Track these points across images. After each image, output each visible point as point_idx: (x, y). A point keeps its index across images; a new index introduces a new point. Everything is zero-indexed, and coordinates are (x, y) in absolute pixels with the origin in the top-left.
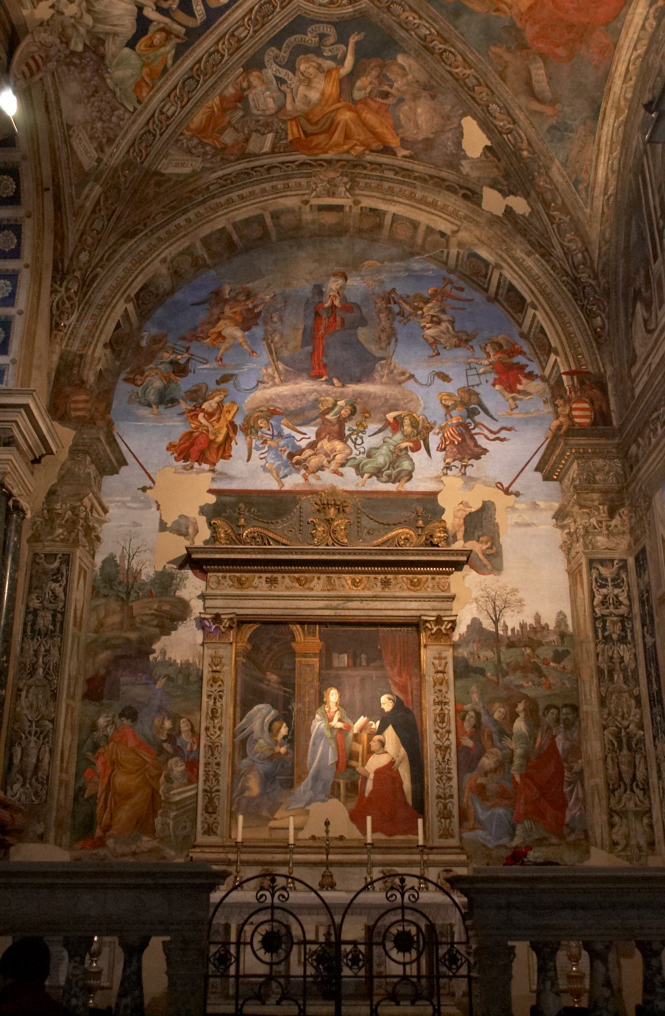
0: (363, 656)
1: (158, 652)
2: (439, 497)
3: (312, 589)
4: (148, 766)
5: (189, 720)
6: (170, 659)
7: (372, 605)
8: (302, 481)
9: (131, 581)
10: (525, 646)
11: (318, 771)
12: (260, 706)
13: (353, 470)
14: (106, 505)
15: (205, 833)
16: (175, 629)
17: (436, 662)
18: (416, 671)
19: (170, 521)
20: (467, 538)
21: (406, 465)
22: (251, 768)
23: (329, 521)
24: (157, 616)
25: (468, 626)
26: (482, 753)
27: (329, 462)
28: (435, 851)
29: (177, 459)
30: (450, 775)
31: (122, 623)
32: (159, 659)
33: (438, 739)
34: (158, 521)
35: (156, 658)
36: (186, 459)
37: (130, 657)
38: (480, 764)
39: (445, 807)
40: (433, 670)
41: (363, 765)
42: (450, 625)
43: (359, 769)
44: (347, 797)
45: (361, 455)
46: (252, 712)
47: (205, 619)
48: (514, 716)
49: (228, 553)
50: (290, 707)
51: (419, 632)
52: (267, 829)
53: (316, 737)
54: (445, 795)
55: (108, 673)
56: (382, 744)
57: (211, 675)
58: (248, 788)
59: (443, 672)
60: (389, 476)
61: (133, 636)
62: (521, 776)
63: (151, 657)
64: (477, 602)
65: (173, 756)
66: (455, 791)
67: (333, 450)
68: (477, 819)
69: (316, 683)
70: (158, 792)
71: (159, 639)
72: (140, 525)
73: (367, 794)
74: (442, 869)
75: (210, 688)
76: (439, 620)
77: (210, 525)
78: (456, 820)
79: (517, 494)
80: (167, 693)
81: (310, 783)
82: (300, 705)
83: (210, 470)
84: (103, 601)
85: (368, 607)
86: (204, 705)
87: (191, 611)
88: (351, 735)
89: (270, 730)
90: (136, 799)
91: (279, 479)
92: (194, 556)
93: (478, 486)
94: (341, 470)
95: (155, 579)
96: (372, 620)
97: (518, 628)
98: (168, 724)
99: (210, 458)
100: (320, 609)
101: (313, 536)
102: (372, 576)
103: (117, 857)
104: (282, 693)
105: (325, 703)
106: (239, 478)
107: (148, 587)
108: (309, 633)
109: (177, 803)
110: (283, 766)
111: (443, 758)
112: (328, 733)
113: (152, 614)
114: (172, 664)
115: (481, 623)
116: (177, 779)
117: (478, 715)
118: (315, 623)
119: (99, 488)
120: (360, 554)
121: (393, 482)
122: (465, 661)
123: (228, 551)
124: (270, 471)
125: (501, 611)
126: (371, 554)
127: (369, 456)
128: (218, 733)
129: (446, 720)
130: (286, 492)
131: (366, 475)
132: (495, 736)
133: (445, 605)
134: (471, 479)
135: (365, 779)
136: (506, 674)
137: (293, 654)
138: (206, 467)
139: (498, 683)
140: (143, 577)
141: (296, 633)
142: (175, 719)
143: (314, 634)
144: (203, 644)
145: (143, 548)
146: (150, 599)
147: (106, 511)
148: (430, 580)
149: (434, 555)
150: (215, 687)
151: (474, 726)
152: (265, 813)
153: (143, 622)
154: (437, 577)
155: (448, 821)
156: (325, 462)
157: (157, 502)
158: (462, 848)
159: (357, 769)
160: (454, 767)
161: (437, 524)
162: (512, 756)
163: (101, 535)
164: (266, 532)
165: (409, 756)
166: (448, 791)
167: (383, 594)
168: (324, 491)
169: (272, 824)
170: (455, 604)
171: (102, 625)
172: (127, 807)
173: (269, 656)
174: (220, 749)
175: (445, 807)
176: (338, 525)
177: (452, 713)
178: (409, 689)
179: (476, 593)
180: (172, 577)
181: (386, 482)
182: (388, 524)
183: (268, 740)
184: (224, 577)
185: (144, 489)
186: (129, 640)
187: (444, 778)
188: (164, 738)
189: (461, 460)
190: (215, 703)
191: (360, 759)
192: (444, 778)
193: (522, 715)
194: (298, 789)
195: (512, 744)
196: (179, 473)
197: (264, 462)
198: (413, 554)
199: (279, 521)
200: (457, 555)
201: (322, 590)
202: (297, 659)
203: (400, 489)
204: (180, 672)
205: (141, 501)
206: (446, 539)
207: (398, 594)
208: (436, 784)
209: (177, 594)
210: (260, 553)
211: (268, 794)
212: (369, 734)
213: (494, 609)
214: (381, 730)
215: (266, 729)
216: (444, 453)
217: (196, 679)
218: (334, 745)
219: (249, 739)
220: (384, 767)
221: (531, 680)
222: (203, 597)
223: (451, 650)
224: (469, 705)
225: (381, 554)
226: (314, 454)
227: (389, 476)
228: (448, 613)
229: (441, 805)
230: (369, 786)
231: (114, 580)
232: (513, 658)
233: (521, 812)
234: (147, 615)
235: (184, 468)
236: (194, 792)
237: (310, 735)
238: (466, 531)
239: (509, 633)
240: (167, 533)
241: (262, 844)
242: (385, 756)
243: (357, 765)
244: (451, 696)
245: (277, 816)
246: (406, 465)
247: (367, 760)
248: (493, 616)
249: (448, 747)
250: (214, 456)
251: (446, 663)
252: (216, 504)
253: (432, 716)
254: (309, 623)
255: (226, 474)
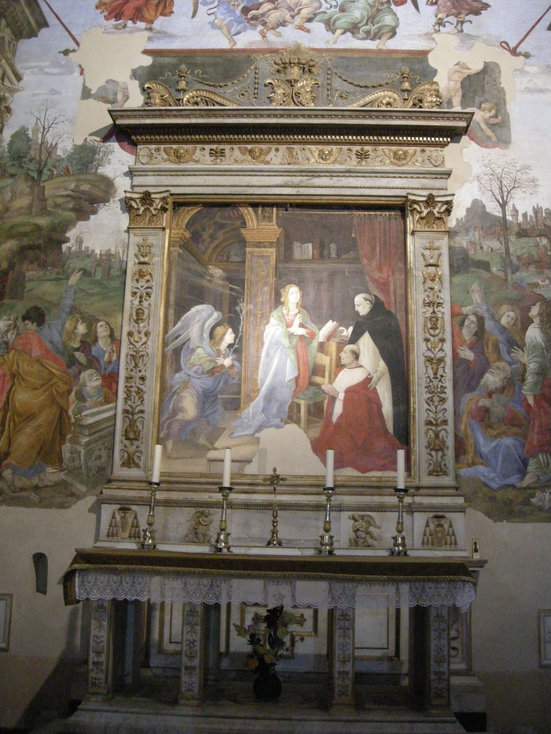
0: (333, 246)
1: (72, 241)
2: (430, 57)
3: (268, 163)
4: (55, 380)
5: (108, 324)
6: (87, 248)
7: (345, 181)
8: (259, 38)
9: (44, 157)
10: (540, 235)
11: (272, 390)
12: (199, 307)
13: (322, 26)
14: (21, 71)
15: (123, 465)
16: (95, 212)
17: (427, 253)
18: (401, 265)
19: (94, 87)
20: (464, 102)
21: (388, 20)
22: (186, 384)
23: (291, 83)
24: (73, 198)
25: (468, 210)
26: (485, 367)
27: (293, 17)
28: (422, 491)
29: (106, 18)
30: (443, 395)
31: (30, 206)
32: (73, 249)
33: (429, 349)
34: (80, 88)
35: (69, 248)
36: (118, 17)
37: (38, 247)
38: (483, 381)
39: (437, 435)
40: (424, 263)
41: (331, 382)
42: (445, 207)
43: (326, 387)
44: (309, 422)
45: (333, 9)
46: (188, 314)
47: (131, 199)
48: (526, 322)
49: (161, 116)
50: (238, 309)
51: (404, 217)
52: (205, 461)
53: (269, 347)
54: (436, 420)
55: (11, 266)
56: (356, 355)
57: (138, 267)
58: (182, 410)
59: (436, 266)
60: (368, 33)
61: (43, 221)
62: (535, 396)
63: (64, 247)
64: (478, 180)
65: (86, 368)
66: (450, 416)
67: (297, 5)
68: (478, 453)
69: (272, 280)
70: (67, 412)
71: (74, 225)
72: (60, 93)
73: (334, 419)
74: (432, 514)
75: (136, 285)
76: (430, 201)
77: (144, 90)
78: (450, 453)
79: (527, 56)
80: (82, 290)
81: (261, 405)
82: (251, 306)
83: (146, 29)
84: (9, 181)
85: (339, 184)
86: (127, 304)
87: (116, 191)
88: (315, 344)
89: (212, 336)
90: (41, 419)
91: (231, 36)
92: (119, 122)
93: (478, 44)
94: (307, 25)
95: (73, 154)
96: (346, 200)
97: (530, 213)
98: (82, 329)
99: (147, 16)
100: (277, 186)
101: (271, 100)
102: (345, 148)
103: (14, 492)
104: (228, 291)
105: (282, 304)
106: (181, 37)
107: (64, 165)
108: (264, 217)
109: (91, 426)
110: (226, 382)
111: (435, 374)
112: (285, 342)
113: (68, 196)
114: (89, 255)
115: (484, 207)
116: (91, 397)
117: (481, 320)
118: (272, 205)
119: (14, 53)
120: (330, 116)
121: (372, 39)
122: (464, 252)
123: (161, 114)
124: (219, 28)
125: (509, 192)
126: (343, 117)
127: (342, 10)
128: (144, 339)
129: (439, 326)
130: (238, 51)
131: (339, 32)
132: (503, 348)
133: (438, 183)
134: (469, 37)
135: (333, 399)
136: (515, 270)
137: (243, 242)
138: (141, 25)
139: (506, 280)
140: (59, 152)
141: (247, 218)
142: (91, 322)
143: (270, 219)
144: (128, 231)
145: (61, 119)
146: (67, 178)
147: (19, 78)
148: (418, 152)
149: (424, 118)
150: (142, 282)
151: (476, 334)
152: (202, 441)
153: (56, 206)
154: (428, 149)
155: (440, 453)
156: (288, 17)
157: (80, 66)
158: (457, 489)
159: (323, 387)
160: (448, 384)
161: (427, 86)
162: (525, 371)
163: (12, 106)
164: (213, 97)
165: (390, 372)
166: (440, 415)
167: (359, 168)
168: (285, 50)
169: (212, 454)
170: (451, 183)
171: (7, 210)
172: (28, 430)
173: (213, 246)
174: (145, 357)
175: (437, 435)
176: (303, 87)
177: (447, 318)
178: (392, 288)
179: (477, 169)
180: (93, 151)
181: (363, 39)
182: (366, 87)
183: (209, 349)
184: (158, 150)
185: (66, 52)
186: (38, 228)
187: (436, 399)
188: (76, 345)
189: (457, 15)
190: (140, 302)
191: (327, 374)
192: (436, 399)
193: (537, 321)
194: (246, 411)
195: (524, 357)
196: (109, 33)
197: (212, 17)
198: (397, 118)
199: (230, 84)
200: (454, 119)
201: (281, 164)
202: (248, 250)
203: (381, 47)
204: (99, 265)
205: (62, 66)
206: (440, 105)
207: (378, 168)
208: (426, 406)
209: (99, 171)
210: (202, 116)
211: (207, 416)
212: (338, 343)
213: (501, 189)
214: (355, 338)
215: (206, 335)
216: (435, 7)
217: (118, 273)
218: (293, 356)
219: (185, 347)
220: (358, 385)
221: (548, 278)
222: (131, 173)
223: (446, 238)
224: (469, 308)
225: (357, 117)
226: (275, 8)
227: (368, 33)
228: (442, 192)
229: (431, 432)
230: (338, 409)
231: (26, 157)
232: (525, 250)
233: (535, 443)
234: (63, 196)
235: (116, 27)
236: (111, 413)
237: (263, 344)
238: (463, 96)
239: (520, 219)
240: (91, 100)
241: (197, 480)
242: (359, 370)
243: (323, 381)
244: (446, 296)
245: (217, 445)
246: (388, 20)
247: (336, 375)
248: (499, 197)
249: (441, 360)
250: (152, 13)
251: (440, 255)
252: (153, 66)
253: (421, 320)
254: (265, 205)
255: (165, 33)
